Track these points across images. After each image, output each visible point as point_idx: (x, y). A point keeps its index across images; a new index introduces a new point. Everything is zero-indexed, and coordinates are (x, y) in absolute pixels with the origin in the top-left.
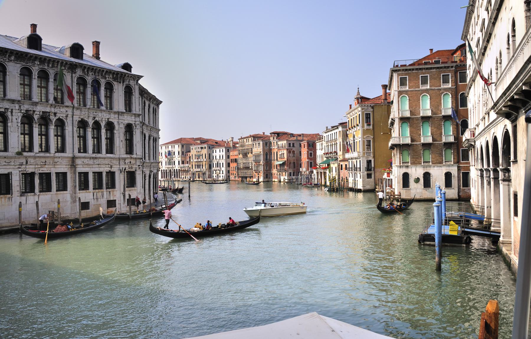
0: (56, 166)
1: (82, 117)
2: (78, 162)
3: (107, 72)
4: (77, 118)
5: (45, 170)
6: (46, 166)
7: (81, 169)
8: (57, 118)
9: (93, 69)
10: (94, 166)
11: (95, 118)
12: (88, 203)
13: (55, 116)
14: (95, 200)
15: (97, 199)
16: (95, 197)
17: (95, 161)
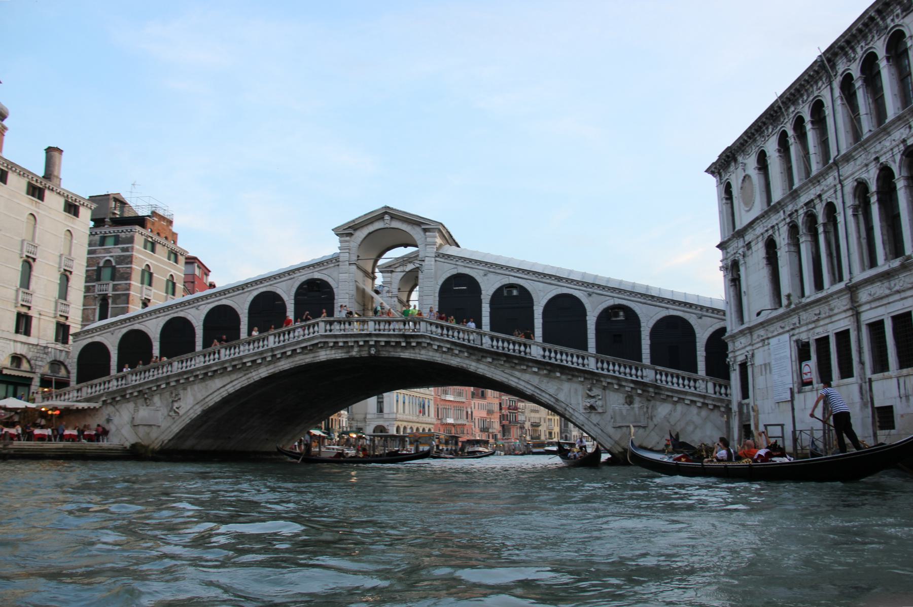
0: (834, 319)
1: (857, 176)
2: (863, 296)
3: (879, 12)
4: (849, 185)
5: (820, 332)
6: (822, 323)
7: (869, 316)
8: (824, 203)
9: (854, 36)
10: (891, 299)
11: (877, 159)
12: (891, 407)
13: (821, 201)
14: (904, 399)
15: (907, 397)
16: (902, 391)
17: (892, 283)
